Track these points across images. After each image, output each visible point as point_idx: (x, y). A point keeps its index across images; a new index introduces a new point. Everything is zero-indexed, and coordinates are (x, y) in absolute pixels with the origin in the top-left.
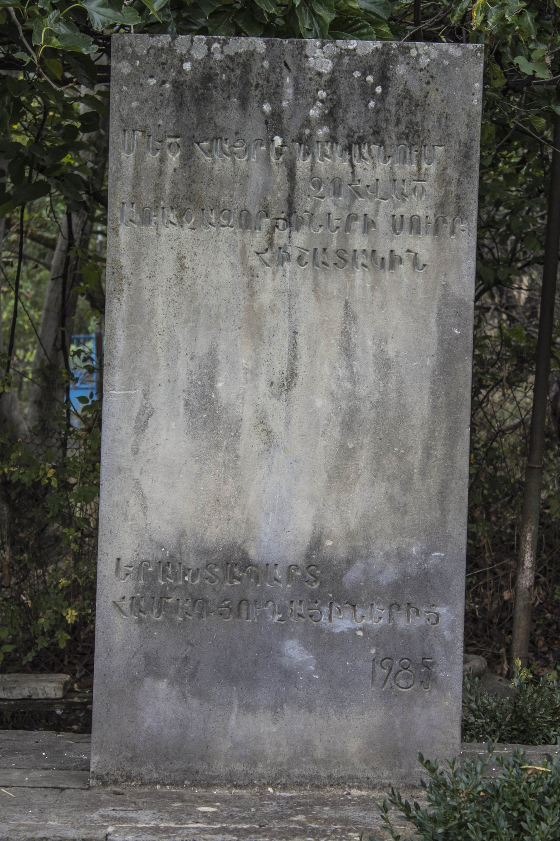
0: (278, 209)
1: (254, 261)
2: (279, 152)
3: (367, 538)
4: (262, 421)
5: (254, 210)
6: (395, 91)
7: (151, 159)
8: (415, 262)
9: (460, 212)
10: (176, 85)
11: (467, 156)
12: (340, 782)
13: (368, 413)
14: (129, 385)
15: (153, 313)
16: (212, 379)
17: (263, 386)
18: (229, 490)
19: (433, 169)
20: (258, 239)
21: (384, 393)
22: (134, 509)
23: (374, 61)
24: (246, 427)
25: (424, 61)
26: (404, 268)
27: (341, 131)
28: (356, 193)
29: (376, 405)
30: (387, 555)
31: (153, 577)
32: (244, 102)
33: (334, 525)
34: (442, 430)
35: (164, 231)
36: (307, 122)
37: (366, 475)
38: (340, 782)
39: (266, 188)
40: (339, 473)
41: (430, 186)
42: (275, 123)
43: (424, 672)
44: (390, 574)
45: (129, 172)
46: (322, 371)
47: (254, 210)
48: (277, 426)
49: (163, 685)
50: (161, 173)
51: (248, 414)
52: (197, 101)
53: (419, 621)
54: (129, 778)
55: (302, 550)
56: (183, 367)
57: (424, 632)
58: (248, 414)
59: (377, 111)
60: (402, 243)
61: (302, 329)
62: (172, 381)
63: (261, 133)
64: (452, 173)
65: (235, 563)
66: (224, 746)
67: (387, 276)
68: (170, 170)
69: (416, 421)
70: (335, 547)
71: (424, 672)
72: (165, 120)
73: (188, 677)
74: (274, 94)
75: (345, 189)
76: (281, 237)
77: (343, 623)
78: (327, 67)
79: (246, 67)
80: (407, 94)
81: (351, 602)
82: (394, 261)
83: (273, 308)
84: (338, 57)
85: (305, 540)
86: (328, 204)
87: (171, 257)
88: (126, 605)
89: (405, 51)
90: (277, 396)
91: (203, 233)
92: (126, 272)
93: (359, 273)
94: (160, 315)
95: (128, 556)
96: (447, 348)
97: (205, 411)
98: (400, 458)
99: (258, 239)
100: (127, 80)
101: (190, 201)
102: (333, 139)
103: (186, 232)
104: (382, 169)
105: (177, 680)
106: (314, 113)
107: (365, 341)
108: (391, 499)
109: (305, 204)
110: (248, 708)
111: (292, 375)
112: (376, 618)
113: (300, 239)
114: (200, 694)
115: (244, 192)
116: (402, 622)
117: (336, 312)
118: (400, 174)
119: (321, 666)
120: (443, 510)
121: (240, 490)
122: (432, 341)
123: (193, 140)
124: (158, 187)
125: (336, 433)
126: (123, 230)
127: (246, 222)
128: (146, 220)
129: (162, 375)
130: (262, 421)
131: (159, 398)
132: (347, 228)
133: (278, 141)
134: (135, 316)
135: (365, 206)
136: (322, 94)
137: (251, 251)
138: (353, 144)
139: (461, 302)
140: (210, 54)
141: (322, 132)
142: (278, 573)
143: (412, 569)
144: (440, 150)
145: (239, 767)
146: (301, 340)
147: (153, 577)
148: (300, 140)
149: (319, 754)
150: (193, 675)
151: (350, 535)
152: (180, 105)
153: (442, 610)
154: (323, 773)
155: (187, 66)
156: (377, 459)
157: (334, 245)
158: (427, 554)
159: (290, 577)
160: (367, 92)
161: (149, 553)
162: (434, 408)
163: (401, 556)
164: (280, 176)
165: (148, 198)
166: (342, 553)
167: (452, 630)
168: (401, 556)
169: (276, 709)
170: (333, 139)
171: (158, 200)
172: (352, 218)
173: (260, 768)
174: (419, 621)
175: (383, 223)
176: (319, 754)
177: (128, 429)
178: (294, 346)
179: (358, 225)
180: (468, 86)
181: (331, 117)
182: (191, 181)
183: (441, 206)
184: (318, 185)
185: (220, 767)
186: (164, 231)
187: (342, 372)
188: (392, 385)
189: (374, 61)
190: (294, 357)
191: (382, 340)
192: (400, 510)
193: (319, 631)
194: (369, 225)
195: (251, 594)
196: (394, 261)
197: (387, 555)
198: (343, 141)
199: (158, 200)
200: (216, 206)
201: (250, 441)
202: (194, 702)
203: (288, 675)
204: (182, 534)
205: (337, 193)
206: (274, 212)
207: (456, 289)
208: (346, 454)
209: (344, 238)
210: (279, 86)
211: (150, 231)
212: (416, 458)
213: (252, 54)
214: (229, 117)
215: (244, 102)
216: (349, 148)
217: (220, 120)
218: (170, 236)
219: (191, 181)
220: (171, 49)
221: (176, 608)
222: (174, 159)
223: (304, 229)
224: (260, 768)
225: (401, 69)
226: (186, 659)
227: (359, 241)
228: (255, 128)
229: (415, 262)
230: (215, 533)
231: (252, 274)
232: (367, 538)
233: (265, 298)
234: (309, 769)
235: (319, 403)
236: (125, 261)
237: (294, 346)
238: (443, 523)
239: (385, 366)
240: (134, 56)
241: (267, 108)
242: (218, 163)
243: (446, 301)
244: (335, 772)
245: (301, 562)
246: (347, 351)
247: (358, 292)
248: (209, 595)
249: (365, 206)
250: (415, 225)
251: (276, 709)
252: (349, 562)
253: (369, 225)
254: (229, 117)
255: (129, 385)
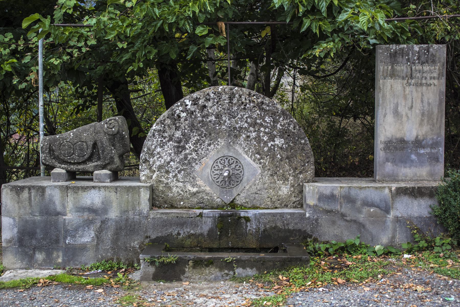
0: (409, 76)
1: (405, 86)
2: (409, 65)
3: (426, 136)
4: (407, 115)
5: (405, 76)
6: (430, 53)
7: (386, 67)
8: (434, 85)
9: (443, 76)
10: (390, 54)
11: (444, 65)
12: (422, 180)
13: (426, 113)
14: (382, 109)
15: (386, 96)
16: (397, 107)
17: (407, 108)
18: (401, 127)
19: (437, 68)
20: (405, 81)
21: (429, 109)
22: (384, 132)
23: (426, 48)
24: (404, 116)
25: (435, 48)
26: (432, 86)
27: (420, 61)
28: (423, 73)
29: (427, 111)
30: (430, 139)
31: (387, 144)
32: (402, 56)
33: (420, 133)
34: (440, 115)
35: (388, 81)
36: (414, 60)
37: (426, 124)
38: (422, 180)
39: (407, 72)
40: (421, 124)
41: (437, 71)
42: (408, 60)
43: (437, 160)
44: (430, 142)
45: (382, 70)
46: (418, 105)
47: (405, 76)
48: (409, 116)
49: (389, 164)
50: (388, 70)
51: (404, 114)
52: (394, 57)
53: (436, 151)
54: (384, 180)
55: (414, 138)
56: (392, 106)
57: (437, 152)
58: (404, 114)
59: (427, 57)
60: (432, 81)
61: (414, 98)
62: (390, 108)
63: (406, 62)
64: (441, 68)
65: (402, 141)
66: (401, 174)
67: (429, 88)
68: (389, 69)
69: (435, 114)
70: (420, 137)
71: (437, 160)
72: (388, 60)
73: (394, 162)
74: (408, 55)
75: (421, 72)
76: (410, 81)
77: (422, 151)
78: (418, 50)
79: (403, 50)
80: (432, 54)
81: (424, 147)
82: (431, 85)
83: (408, 94)
84: (420, 48)
85: (415, 136)
86: (418, 75)
87: (389, 85)
88: (382, 149)
89: (432, 46)
90: (409, 110)
91: (395, 81)
92: (382, 88)
93: (424, 87)
94: (388, 96)
95: (383, 140)
96: (440, 100)
97: (396, 113)
98: (432, 121)
99: (405, 81)
100: (381, 53)
101: (393, 75)
102: (419, 63)
103: (392, 81)
104: (428, 68)
105: (392, 163)
106: (415, 58)
107: (425, 100)
108: (431, 128)
109: (414, 75)
110: (405, 167)
111: (412, 106)
112: (428, 150)
113: (413, 81)
114: (396, 165)
115: (403, 73)
116: (433, 151)
117: (420, 94)
118: (431, 69)
119: (418, 159)
120: (440, 130)
121: (403, 127)
122: (438, 99)
123: (393, 64)
124: (387, 73)
125: (420, 117)
126: (381, 81)
127: (403, 78)
128: (385, 79)
129: (388, 107)
130: (407, 115)
131: (388, 111)
132: (422, 79)
133: (409, 63)
134: (384, 96)
135: (425, 75)
136: (417, 55)
137: (404, 84)
138: (423, 63)
139: (443, 92)
140: (396, 48)
141: (417, 61)
142: (410, 143)
143: (435, 141)
144: (439, 64)
145: (404, 178)
146: (414, 100)
147: (387, 144)
148: (413, 63)
149: (418, 175)
150: (395, 161)
151: (423, 135)
152: (391, 57)
153: (440, 148)
154: (419, 179)
155: (392, 50)
156: (428, 121)
157: (419, 82)
158: (437, 138)
159: (412, 143)
160: (425, 54)
161: (386, 140)
162: (438, 112)
163: (433, 139)
164: (409, 70)
165: (385, 75)
166: (422, 139)
167: (442, 152)
168: (433, 139)
169: (410, 167)
170: (419, 63)
171: (387, 75)
172: (423, 77)
173: (407, 178)
174: (436, 151)
175: (428, 78)
176: (418, 175)
177: (382, 117)
178: (412, 101)
179: (424, 78)
180: (444, 52)
181: (419, 59)
182: (393, 71)
183: (439, 74)
184: (416, 71)
185: (400, 178)
186: (388, 81)
187: (421, 105)
188: (431, 107)
189: (426, 48)
190: (412, 103)
191: (428, 99)
192: (432, 130)
193: (418, 153)
194: (426, 78)
195: (405, 147)
196: (431, 85)
197: (430, 139)
198: (421, 63)
199: (387, 75)
200: (398, 76)
201: (405, 119)
202: (395, 166)
203: (412, 161)
204: (392, 136)
205: (420, 73)
206: (408, 76)
207: (442, 89)
208: (422, 120)
209: (421, 81)
210: (409, 53)
211: (386, 81)
212: (435, 121)
213: (404, 48)
214: (400, 59)
215: (402, 56)
216: (422, 64)
217: (398, 60)
218: (389, 82)
219: (393, 71)
220: (389, 47)
221: (391, 149)
222: (390, 67)
223: (414, 79)
224: (407, 178)
225: (431, 50)
226: (394, 159)
227: (424, 81)
228: (405, 61)
229: (434, 85)
230: (399, 135)
231: (404, 88)
232: (426, 136)
233: (407, 92)
234: (416, 178)
235: (417, 111)
236: (381, 86)
237: (412, 101)
238: (440, 132)
239: (429, 104)
240: (382, 49)
241: (407, 57)
242: (398, 68)
243: (440, 92)
244: (421, 178)
245: (414, 140)
246: (422, 102)
247: (424, 91)
248: (398, 147)
249: (425, 75)
250: (434, 78)
251: (410, 167)
252: (423, 140)
253: (426, 78)
254: (400, 59)
255: (382, 109)
